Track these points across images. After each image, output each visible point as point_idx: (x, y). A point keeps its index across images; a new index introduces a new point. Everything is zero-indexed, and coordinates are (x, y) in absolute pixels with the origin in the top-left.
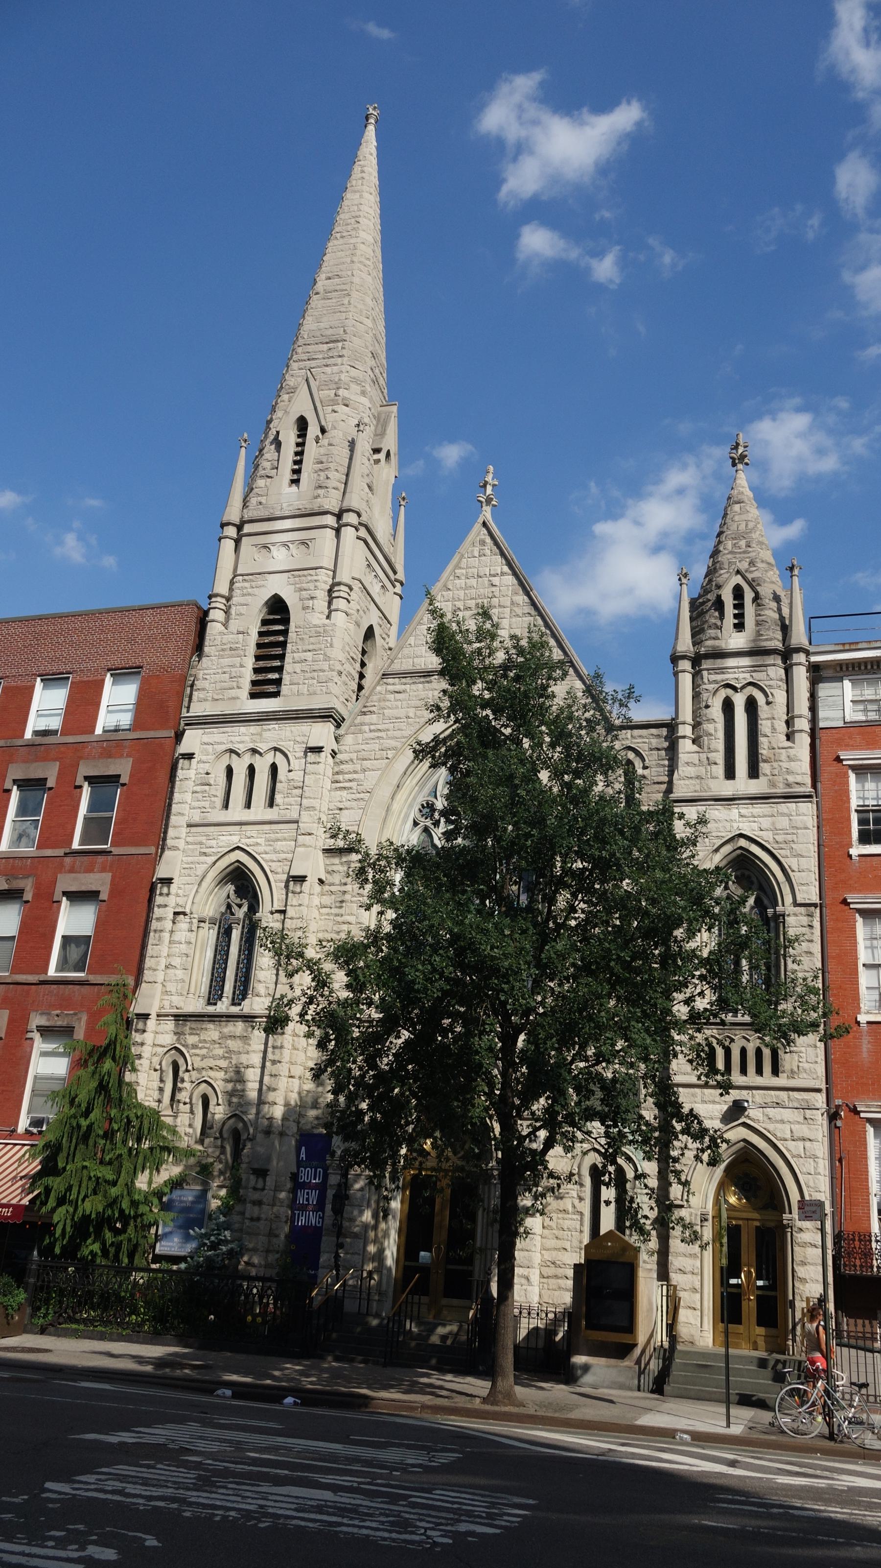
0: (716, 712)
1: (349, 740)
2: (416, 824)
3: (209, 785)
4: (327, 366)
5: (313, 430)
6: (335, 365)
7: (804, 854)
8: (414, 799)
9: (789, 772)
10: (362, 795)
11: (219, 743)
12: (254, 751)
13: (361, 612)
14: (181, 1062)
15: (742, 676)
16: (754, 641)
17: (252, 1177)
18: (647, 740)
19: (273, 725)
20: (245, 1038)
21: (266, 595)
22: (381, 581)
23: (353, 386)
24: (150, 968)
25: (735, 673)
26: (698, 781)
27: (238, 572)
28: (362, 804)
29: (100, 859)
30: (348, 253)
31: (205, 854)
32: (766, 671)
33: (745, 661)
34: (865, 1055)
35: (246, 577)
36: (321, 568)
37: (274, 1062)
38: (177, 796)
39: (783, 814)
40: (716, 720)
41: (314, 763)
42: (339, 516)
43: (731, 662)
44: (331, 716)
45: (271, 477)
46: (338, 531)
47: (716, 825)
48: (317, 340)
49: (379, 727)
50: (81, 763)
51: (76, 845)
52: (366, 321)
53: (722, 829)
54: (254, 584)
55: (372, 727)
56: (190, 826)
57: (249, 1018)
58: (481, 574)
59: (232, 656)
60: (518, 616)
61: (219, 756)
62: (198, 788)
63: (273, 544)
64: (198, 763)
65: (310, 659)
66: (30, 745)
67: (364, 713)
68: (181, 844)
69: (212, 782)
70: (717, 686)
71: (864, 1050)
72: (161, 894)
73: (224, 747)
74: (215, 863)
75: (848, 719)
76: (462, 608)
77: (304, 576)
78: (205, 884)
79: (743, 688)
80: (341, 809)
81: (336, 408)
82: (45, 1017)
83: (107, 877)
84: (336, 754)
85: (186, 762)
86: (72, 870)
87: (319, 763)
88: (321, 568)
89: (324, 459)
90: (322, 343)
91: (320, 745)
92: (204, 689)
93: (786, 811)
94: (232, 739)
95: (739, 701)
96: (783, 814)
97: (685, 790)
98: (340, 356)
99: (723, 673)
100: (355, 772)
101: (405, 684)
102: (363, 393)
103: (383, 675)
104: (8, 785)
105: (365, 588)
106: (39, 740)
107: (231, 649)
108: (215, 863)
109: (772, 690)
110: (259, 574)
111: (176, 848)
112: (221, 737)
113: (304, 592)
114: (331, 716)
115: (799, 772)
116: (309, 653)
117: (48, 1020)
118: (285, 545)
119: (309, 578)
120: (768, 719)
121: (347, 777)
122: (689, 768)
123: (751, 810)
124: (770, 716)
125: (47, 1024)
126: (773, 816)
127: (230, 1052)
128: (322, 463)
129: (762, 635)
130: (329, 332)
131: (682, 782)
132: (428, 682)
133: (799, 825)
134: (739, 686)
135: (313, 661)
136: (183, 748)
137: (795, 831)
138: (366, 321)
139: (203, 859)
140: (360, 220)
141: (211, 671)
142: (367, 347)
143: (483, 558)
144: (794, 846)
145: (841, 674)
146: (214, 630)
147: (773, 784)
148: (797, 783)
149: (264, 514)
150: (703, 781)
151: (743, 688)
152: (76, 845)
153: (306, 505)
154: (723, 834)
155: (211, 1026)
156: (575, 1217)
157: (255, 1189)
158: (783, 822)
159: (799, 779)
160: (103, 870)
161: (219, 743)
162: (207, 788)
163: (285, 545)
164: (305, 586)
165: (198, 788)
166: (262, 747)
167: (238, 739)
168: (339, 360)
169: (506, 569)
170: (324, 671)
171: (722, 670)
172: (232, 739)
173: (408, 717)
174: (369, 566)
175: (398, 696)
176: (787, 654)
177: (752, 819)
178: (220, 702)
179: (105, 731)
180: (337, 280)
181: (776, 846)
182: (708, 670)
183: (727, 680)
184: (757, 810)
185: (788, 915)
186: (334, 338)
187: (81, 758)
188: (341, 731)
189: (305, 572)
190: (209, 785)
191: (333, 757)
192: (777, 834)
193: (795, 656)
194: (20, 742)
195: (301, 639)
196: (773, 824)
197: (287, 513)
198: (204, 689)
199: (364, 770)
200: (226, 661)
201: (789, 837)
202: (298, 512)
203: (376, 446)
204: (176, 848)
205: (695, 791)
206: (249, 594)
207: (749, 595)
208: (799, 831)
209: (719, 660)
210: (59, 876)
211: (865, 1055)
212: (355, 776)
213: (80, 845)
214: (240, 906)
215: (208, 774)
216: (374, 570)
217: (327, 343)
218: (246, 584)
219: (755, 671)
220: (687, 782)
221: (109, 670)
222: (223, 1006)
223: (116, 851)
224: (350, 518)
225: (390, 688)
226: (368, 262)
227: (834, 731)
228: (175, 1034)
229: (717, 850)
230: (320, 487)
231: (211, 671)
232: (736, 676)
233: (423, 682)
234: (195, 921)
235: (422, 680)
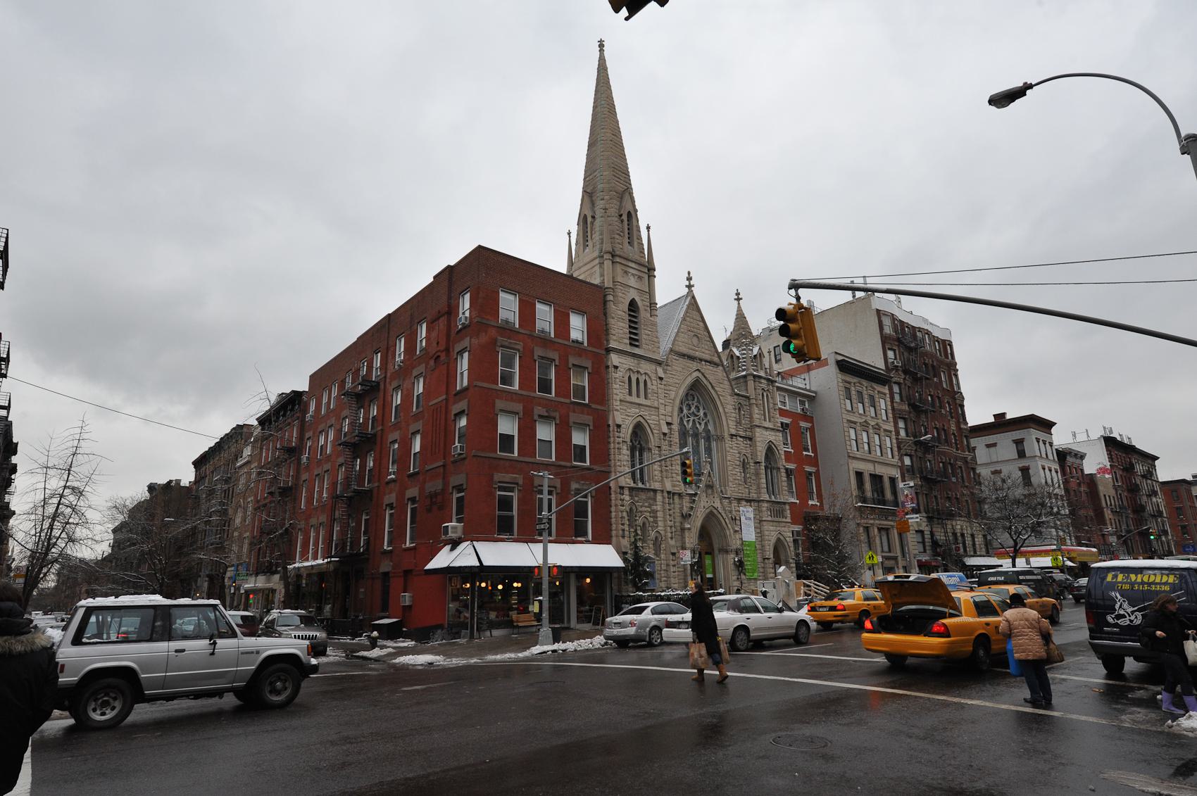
12: (638, 372)
14: (634, 508)
17: (671, 556)
20: (655, 500)
24: (618, 466)
31: (629, 416)
37: (670, 510)
43: (763, 381)
46: (649, 276)
56: (621, 401)
57: (655, 491)
67: (667, 365)
68: (618, 408)
83: (591, 418)
118: (633, 275)
125: (580, 487)
127: (650, 504)
139: (627, 417)
149: (625, 256)
155: (642, 493)
157: (673, 560)
160: (588, 414)
166: (642, 371)
169: (701, 319)
171: (761, 383)
199: (670, 390)
214: (636, 441)
221: (571, 308)
222: (640, 485)
223: (594, 406)
228: (630, 496)
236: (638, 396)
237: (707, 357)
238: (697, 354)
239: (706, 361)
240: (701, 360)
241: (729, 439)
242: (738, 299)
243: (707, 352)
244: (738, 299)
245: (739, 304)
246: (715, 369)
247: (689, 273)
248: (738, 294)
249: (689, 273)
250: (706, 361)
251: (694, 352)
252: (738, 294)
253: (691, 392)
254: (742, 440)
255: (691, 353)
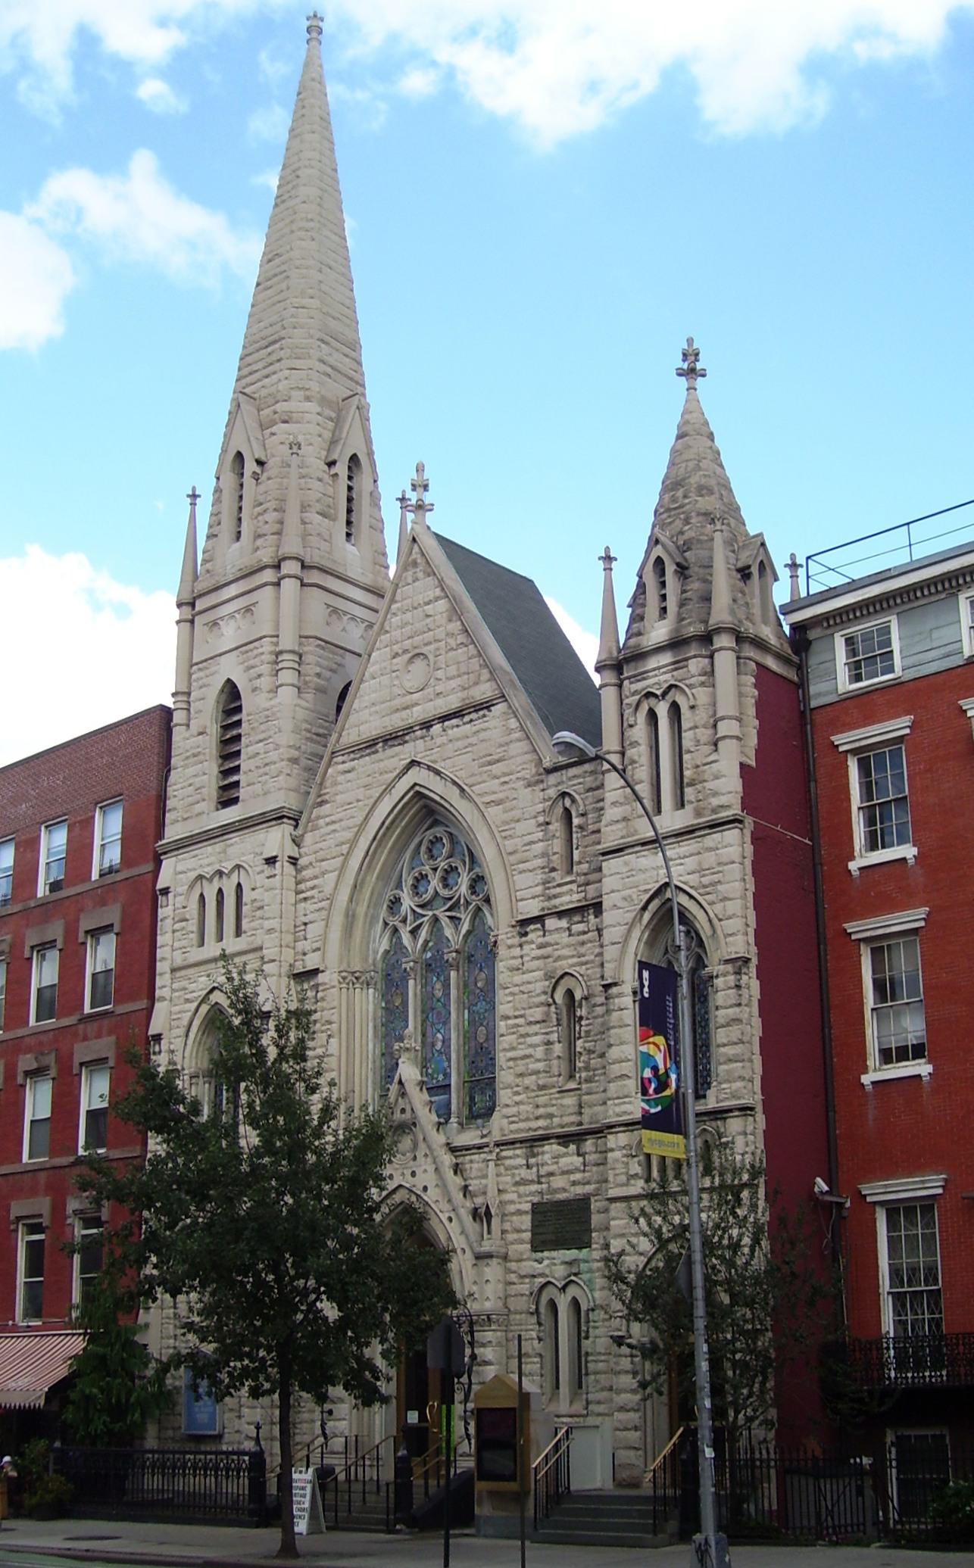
0: (640, 732)
1: (308, 838)
2: (386, 924)
3: (187, 920)
4: (267, 377)
5: (250, 466)
6: (274, 373)
7: (731, 896)
8: (380, 895)
9: (715, 794)
10: (320, 905)
11: (191, 870)
12: (220, 873)
13: (328, 674)
15: (662, 678)
16: (677, 630)
18: (581, 780)
19: (235, 838)
21: (219, 683)
22: (363, 621)
23: (294, 393)
25: (656, 676)
26: (624, 824)
27: (194, 661)
28: (324, 913)
29: (106, 1022)
30: (287, 221)
32: (687, 666)
33: (666, 658)
34: (871, 1122)
35: (200, 666)
36: (265, 637)
38: (160, 940)
39: (710, 849)
40: (640, 741)
41: (271, 877)
42: (277, 567)
44: (283, 817)
45: (216, 536)
47: (643, 876)
48: (257, 346)
49: (333, 818)
50: (82, 916)
51: (87, 1010)
52: (306, 301)
53: (649, 881)
54: (208, 672)
55: (327, 820)
58: (415, 605)
59: (196, 764)
60: (452, 649)
61: (191, 887)
62: (177, 926)
63: (221, 618)
64: (175, 896)
65: (262, 751)
66: (44, 904)
69: (188, 917)
70: (638, 697)
71: (870, 1117)
72: (154, 1053)
73: (193, 875)
74: (197, 1010)
75: (841, 689)
76: (400, 651)
77: (251, 650)
78: (192, 1035)
79: (665, 694)
80: (305, 924)
81: (274, 429)
82: (78, 1201)
84: (296, 859)
85: (164, 898)
86: (85, 1039)
87: (275, 875)
88: (265, 637)
89: (261, 499)
90: (262, 349)
91: (274, 854)
92: (175, 809)
93: (711, 844)
94: (201, 862)
95: (662, 709)
96: (710, 849)
97: (612, 838)
98: (279, 361)
99: (644, 679)
100: (316, 877)
101: (353, 760)
102: (308, 399)
103: (333, 753)
104: (81, 938)
105: (327, 642)
106: (110, 879)
107: (195, 755)
108: (197, 1010)
109: (694, 691)
110: (211, 658)
111: (163, 999)
112: (205, 859)
113: (252, 671)
114: (283, 817)
115: (724, 791)
116: (261, 744)
117: (81, 1203)
119: (255, 652)
120: (690, 729)
121: (309, 884)
122: (616, 809)
123: (677, 850)
124: (692, 725)
126: (699, 853)
128: (261, 504)
129: (683, 619)
130: (270, 330)
131: (609, 828)
132: (374, 753)
133: (725, 860)
134: (658, 692)
135: (266, 753)
136: (160, 885)
137: (720, 869)
138: (306, 301)
140: (299, 173)
141: (179, 786)
142: (312, 337)
143: (416, 584)
144: (719, 887)
145: (829, 632)
146: (177, 735)
147: (698, 813)
148: (722, 806)
150: (630, 823)
151: (665, 694)
152: (87, 1010)
153: (248, 561)
154: (649, 887)
156: (536, 1360)
158: (710, 859)
159: (723, 800)
161: (191, 870)
162: (184, 924)
163: (231, 616)
164: (252, 662)
165: (177, 926)
167: (206, 861)
168: (277, 366)
170: (275, 763)
171: (641, 676)
172: (201, 862)
173: (358, 801)
174: (335, 611)
175: (349, 776)
176: (706, 639)
177: (678, 861)
178: (189, 820)
179: (101, 876)
180: (277, 261)
181: (702, 891)
182: (628, 678)
183: (648, 686)
184: (683, 849)
185: (717, 976)
186: (271, 339)
187: (81, 910)
188: (299, 831)
189: (251, 646)
190: (187, 920)
191: (294, 864)
192: (704, 876)
193: (715, 639)
194: (32, 904)
195: (252, 729)
196: (700, 864)
197: (231, 578)
198: (175, 809)
199: (323, 874)
200: (191, 771)
201: (716, 878)
202: (239, 575)
203: (330, 459)
204: (163, 999)
205: (622, 837)
206: (205, 686)
207: (670, 569)
208: (725, 867)
209: (640, 663)
210: (75, 1046)
211: (871, 1122)
212: (315, 882)
213: (92, 1008)
215: (184, 907)
216: (345, 613)
217: (267, 347)
218: (201, 674)
219: (676, 669)
220: (614, 827)
224: (290, 567)
225: (341, 767)
226: (311, 224)
227: (829, 709)
229: (644, 908)
230: (260, 536)
231: (179, 786)
232: (655, 680)
233: (369, 755)
234: (186, 1077)
235: (368, 751)
236: (220, 938)
237: (453, 702)
238: (418, 714)
239: (444, 718)
240: (427, 725)
241: (516, 940)
242: (691, 373)
243: (453, 683)
244: (691, 373)
245: (691, 389)
246: (479, 725)
247: (420, 469)
248: (691, 355)
249: (420, 469)
250: (444, 718)
251: (404, 714)
252: (691, 355)
253: (429, 835)
254: (564, 923)
255: (397, 721)
